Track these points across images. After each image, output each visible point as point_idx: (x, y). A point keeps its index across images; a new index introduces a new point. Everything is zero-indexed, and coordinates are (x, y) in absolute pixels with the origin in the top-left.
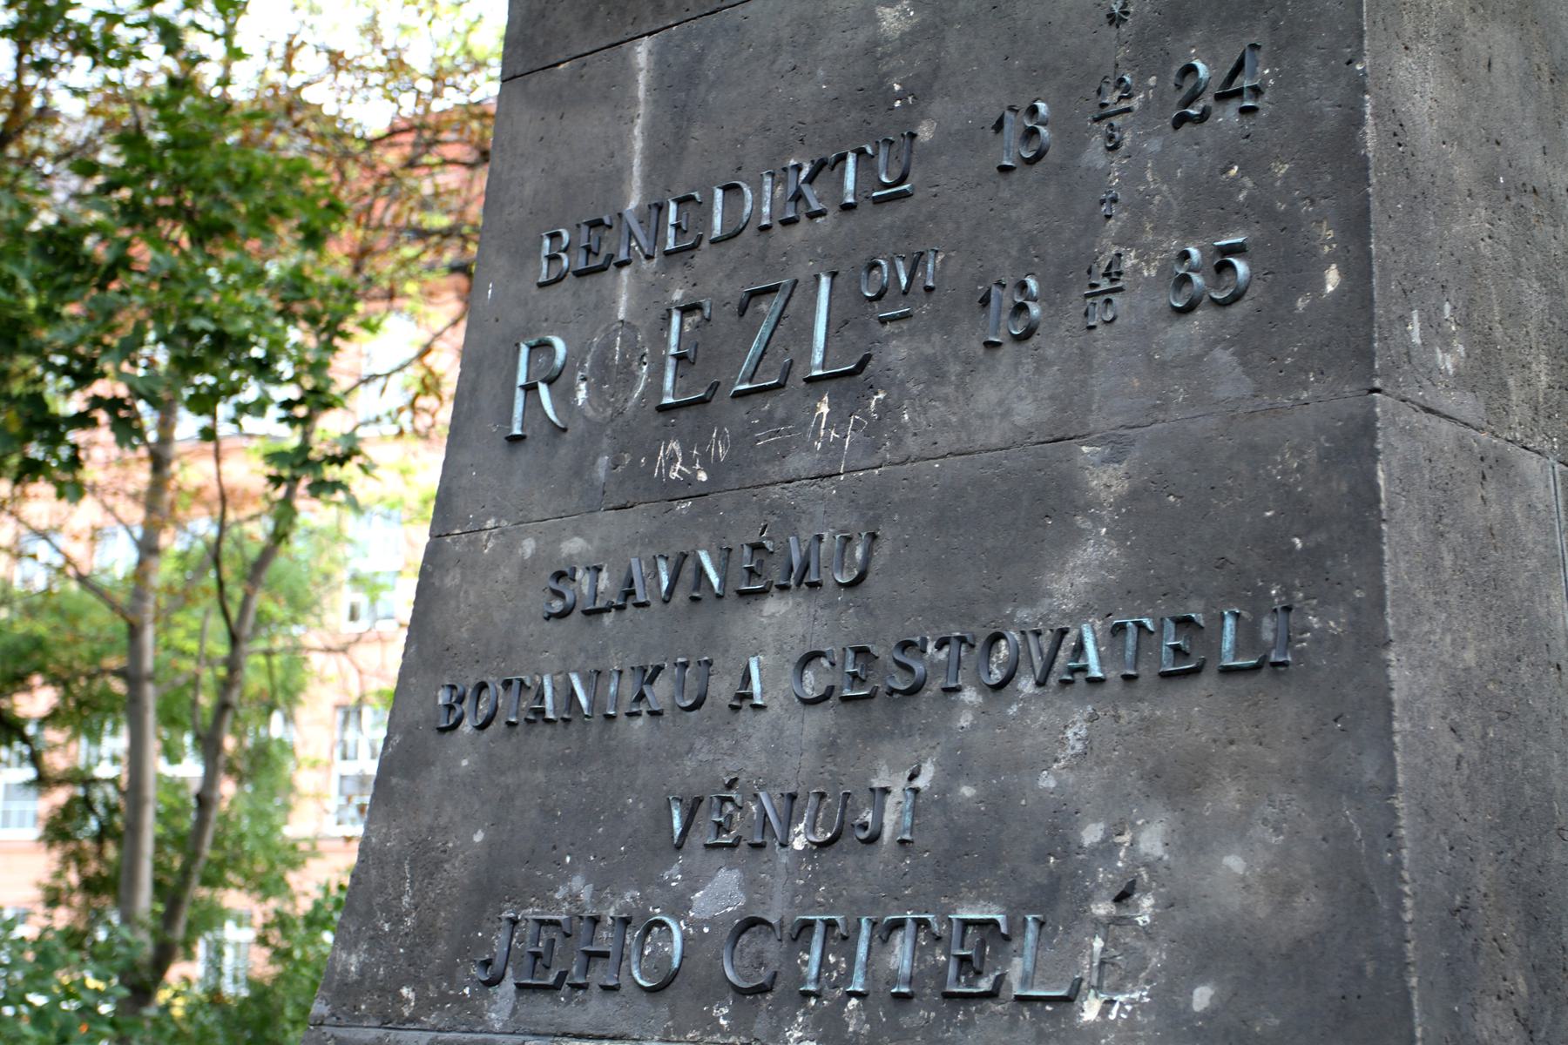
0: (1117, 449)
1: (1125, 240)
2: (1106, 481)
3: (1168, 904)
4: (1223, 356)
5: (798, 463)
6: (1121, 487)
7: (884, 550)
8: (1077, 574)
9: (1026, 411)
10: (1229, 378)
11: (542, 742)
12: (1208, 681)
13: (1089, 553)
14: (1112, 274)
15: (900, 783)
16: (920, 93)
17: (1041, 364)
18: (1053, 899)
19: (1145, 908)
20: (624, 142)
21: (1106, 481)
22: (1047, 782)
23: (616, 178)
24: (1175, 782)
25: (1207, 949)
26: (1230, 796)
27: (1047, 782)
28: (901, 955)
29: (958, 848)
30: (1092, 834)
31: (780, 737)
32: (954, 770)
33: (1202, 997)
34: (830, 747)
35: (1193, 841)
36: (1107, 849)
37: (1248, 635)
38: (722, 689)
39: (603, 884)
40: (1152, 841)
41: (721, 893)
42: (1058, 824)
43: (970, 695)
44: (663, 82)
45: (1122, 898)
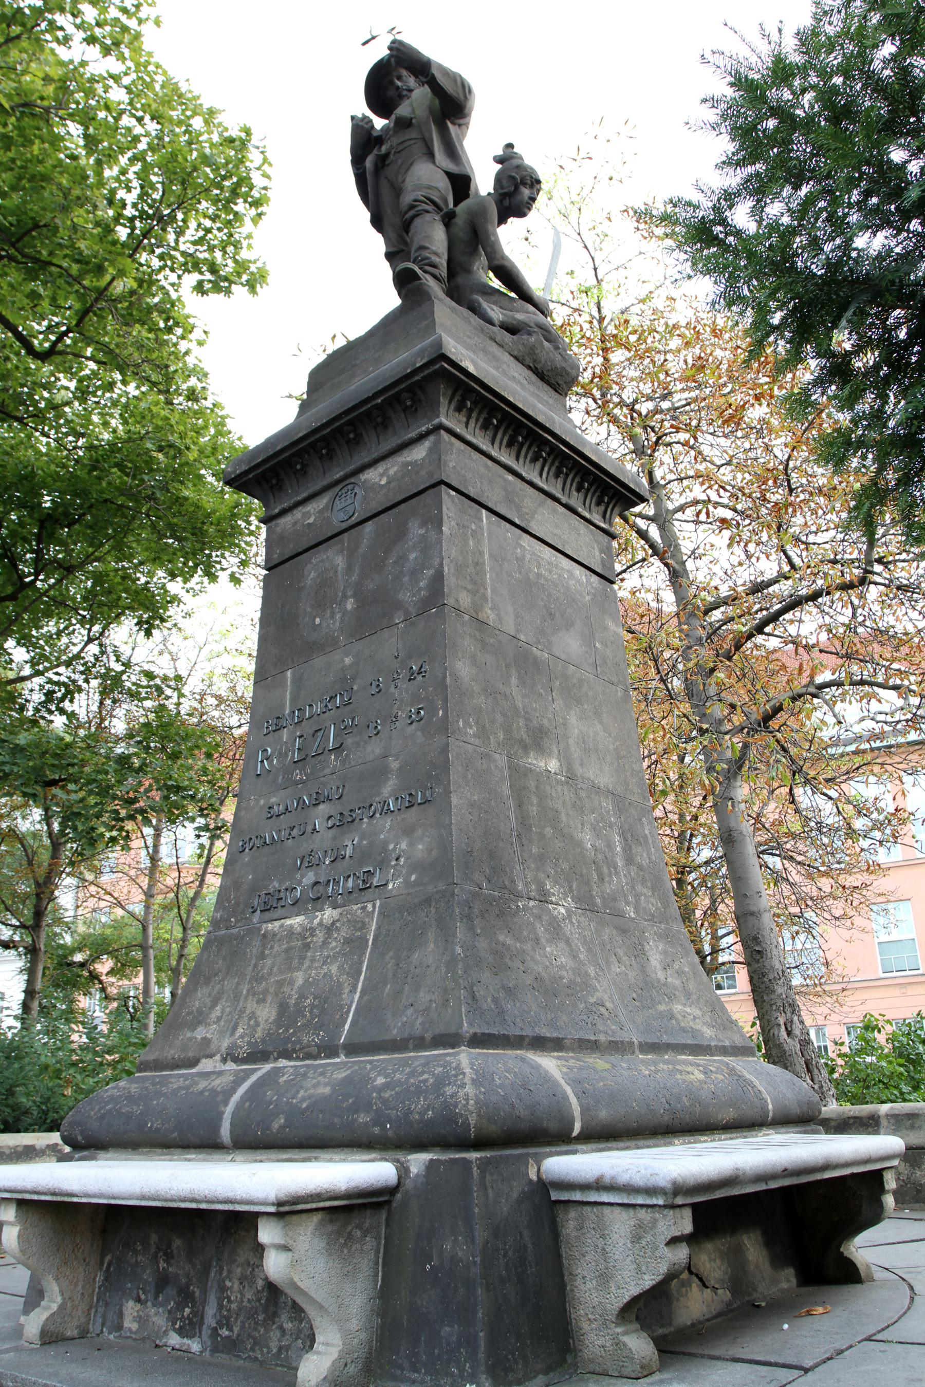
0: (397, 757)
1: (399, 709)
2: (394, 765)
4: (419, 733)
5: (327, 771)
6: (397, 766)
7: (347, 789)
9: (378, 751)
10: (420, 738)
11: (266, 850)
12: (415, 807)
13: (391, 782)
14: (396, 717)
16: (354, 678)
17: (381, 740)
18: (382, 864)
20: (285, 697)
21: (394, 765)
22: (382, 837)
23: (283, 706)
24: (408, 831)
26: (419, 832)
27: (382, 837)
28: (350, 883)
29: (362, 856)
30: (391, 847)
31: (324, 838)
32: (362, 838)
33: (413, 877)
34: (334, 838)
35: (412, 844)
37: (423, 794)
39: (281, 882)
41: (309, 877)
43: (365, 820)
45: (397, 859)
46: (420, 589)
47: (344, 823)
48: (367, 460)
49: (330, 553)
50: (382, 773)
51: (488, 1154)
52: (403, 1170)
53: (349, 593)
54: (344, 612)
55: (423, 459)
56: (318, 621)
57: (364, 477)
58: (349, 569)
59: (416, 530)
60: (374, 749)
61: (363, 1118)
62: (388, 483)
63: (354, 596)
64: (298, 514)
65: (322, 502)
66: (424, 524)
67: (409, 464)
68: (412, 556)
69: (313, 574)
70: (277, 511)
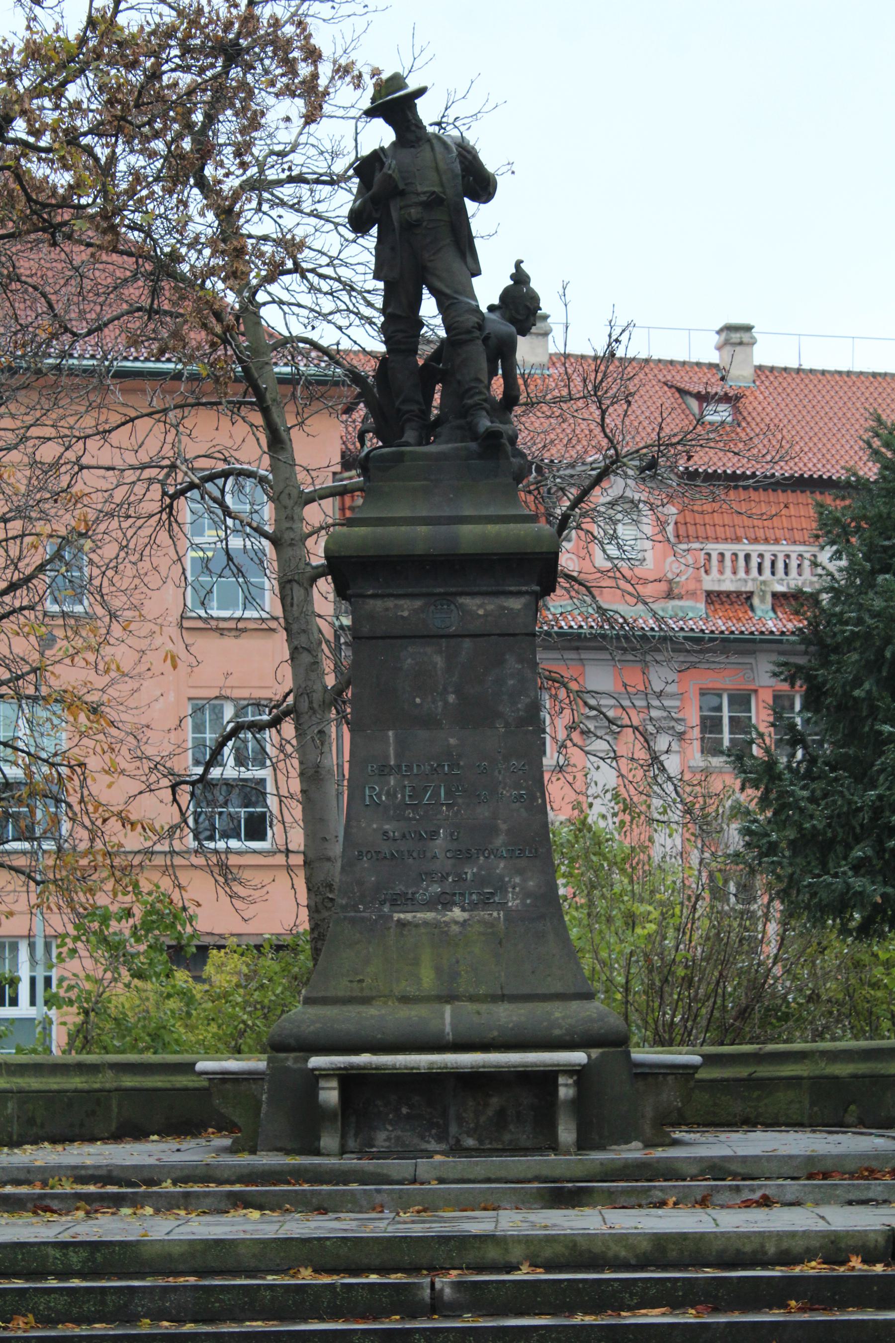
0: (505, 822)
1: (504, 788)
2: (503, 827)
3: (522, 889)
4: (522, 810)
5: (439, 817)
8: (499, 841)
9: (487, 814)
10: (524, 814)
15: (470, 872)
19: (517, 889)
21: (503, 827)
23: (387, 757)
24: (520, 872)
25: (528, 895)
28: (474, 897)
29: (481, 881)
30: (507, 879)
33: (528, 901)
36: (510, 881)
37: (530, 852)
38: (429, 855)
40: (517, 880)
42: (501, 878)
45: (514, 888)
46: (518, 710)
47: (464, 856)
48: (467, 589)
49: (429, 650)
50: (493, 830)
51: (612, 1050)
52: (589, 1057)
53: (450, 690)
54: (446, 703)
55: (519, 610)
56: (418, 700)
57: (461, 600)
59: (512, 664)
60: (483, 812)
61: (557, 1032)
62: (485, 616)
64: (390, 603)
65: (418, 603)
67: (505, 608)
68: (511, 682)
69: (409, 661)
70: (370, 592)
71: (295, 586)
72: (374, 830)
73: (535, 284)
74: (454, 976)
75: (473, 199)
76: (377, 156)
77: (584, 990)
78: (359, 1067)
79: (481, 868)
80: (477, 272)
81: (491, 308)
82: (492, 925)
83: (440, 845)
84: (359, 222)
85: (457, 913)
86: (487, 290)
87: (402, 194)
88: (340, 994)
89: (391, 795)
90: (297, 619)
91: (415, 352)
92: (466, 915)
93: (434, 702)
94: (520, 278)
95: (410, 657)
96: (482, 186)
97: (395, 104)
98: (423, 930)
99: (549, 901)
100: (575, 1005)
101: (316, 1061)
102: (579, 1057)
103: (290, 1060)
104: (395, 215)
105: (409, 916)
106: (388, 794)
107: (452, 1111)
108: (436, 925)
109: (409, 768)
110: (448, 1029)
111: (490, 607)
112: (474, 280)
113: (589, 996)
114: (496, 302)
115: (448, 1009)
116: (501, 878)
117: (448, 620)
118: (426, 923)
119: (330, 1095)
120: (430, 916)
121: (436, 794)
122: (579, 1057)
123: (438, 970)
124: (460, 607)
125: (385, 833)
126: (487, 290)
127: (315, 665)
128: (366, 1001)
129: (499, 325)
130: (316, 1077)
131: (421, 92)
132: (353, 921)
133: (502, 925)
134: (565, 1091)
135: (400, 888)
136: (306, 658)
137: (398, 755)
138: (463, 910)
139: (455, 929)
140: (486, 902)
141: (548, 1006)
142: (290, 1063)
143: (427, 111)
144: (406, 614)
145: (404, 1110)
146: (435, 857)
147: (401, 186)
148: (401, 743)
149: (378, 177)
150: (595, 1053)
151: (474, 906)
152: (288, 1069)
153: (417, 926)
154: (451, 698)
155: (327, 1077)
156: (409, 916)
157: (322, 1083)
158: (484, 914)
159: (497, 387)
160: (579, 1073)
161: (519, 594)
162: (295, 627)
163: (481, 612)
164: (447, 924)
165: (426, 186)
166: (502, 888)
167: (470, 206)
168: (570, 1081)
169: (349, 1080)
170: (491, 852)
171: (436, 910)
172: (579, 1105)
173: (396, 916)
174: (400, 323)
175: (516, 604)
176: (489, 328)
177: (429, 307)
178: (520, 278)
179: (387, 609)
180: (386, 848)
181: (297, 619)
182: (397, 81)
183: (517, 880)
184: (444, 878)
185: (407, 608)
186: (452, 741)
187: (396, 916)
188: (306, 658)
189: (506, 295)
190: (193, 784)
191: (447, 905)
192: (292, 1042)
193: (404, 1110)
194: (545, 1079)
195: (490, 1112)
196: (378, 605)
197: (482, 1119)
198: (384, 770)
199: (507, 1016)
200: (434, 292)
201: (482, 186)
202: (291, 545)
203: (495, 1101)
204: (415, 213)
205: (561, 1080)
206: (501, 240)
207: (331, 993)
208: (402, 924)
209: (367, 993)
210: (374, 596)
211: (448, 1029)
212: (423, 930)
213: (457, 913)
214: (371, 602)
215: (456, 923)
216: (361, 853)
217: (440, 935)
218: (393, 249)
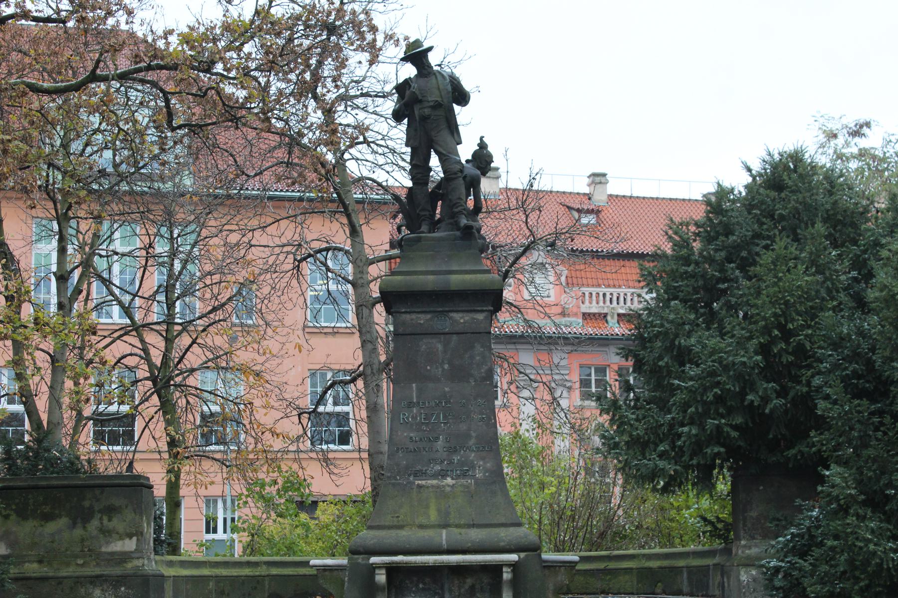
2: (474, 434)
8: (472, 442)
15: (456, 458)
23: (412, 398)
24: (483, 459)
29: (462, 463)
38: (434, 450)
40: (481, 463)
42: (472, 462)
44: (417, 388)
47: (453, 450)
49: (434, 341)
50: (469, 437)
54: (444, 369)
58: (445, 352)
59: (478, 349)
60: (463, 427)
61: (502, 544)
63: (449, 364)
64: (414, 316)
65: (429, 316)
66: (482, 347)
71: (364, 308)
72: (406, 437)
73: (490, 149)
74: (448, 514)
75: (459, 104)
76: (407, 82)
77: (517, 522)
78: (397, 563)
79: (462, 457)
80: (460, 143)
81: (467, 161)
82: (468, 487)
83: (440, 444)
84: (398, 116)
85: (449, 481)
86: (465, 152)
87: (420, 101)
88: (387, 524)
89: (414, 418)
90: (365, 326)
91: (427, 184)
92: (454, 482)
93: (437, 368)
94: (482, 145)
95: (424, 344)
96: (462, 98)
97: (417, 55)
98: (431, 490)
99: (497, 476)
100: (512, 529)
101: (374, 560)
102: (514, 557)
103: (360, 559)
104: (416, 112)
105: (424, 482)
106: (412, 418)
107: (446, 586)
108: (438, 487)
109: (424, 403)
110: (444, 542)
111: (467, 318)
112: (459, 147)
113: (519, 525)
114: (470, 158)
115: (444, 532)
116: (472, 462)
117: (444, 325)
118: (433, 486)
119: (381, 577)
120: (435, 482)
121: (438, 417)
122: (514, 557)
123: (439, 510)
124: (450, 318)
125: (411, 438)
126: (465, 152)
127: (375, 349)
128: (401, 527)
129: (471, 170)
130: (373, 568)
131: (430, 49)
132: (393, 485)
133: (473, 488)
134: (507, 575)
135: (419, 467)
136: (370, 346)
137: (417, 397)
138: (453, 479)
139: (448, 489)
140: (464, 475)
141: (497, 530)
142: (360, 561)
143: (433, 59)
144: (422, 322)
145: (421, 586)
146: (437, 451)
147: (420, 98)
148: (420, 391)
149: (408, 93)
150: (523, 555)
151: (458, 477)
152: (359, 563)
153: (428, 487)
154: (446, 366)
155: (379, 567)
156: (424, 482)
157: (377, 571)
158: (463, 481)
159: (470, 203)
160: (514, 566)
161: (482, 311)
162: (364, 330)
163: (462, 321)
164: (444, 486)
165: (433, 97)
166: (473, 467)
167: (457, 108)
168: (509, 570)
169: (392, 570)
170: (467, 448)
171: (438, 479)
172: (515, 583)
173: (417, 482)
174: (419, 170)
175: (481, 317)
176: (466, 172)
177: (434, 161)
178: (482, 145)
179: (412, 320)
180: (411, 447)
181: (365, 326)
182: (417, 43)
183: (481, 463)
184: (442, 462)
185: (422, 319)
186: (446, 389)
187: (417, 482)
188: (370, 346)
189: (475, 155)
190: (309, 413)
191: (444, 476)
192: (361, 550)
193: (421, 586)
194: (496, 569)
195: (467, 586)
196: (407, 317)
197: (462, 590)
198: (410, 405)
199: (476, 535)
200: (437, 152)
201: (462, 98)
202: (362, 286)
203: (469, 581)
204: (427, 111)
205: (505, 569)
206: (472, 125)
207: (382, 523)
208: (420, 487)
209: (401, 523)
210: (406, 312)
211: (444, 542)
212: (431, 490)
213: (449, 481)
214: (404, 316)
215: (449, 486)
216: (398, 449)
217: (440, 492)
218: (416, 130)
